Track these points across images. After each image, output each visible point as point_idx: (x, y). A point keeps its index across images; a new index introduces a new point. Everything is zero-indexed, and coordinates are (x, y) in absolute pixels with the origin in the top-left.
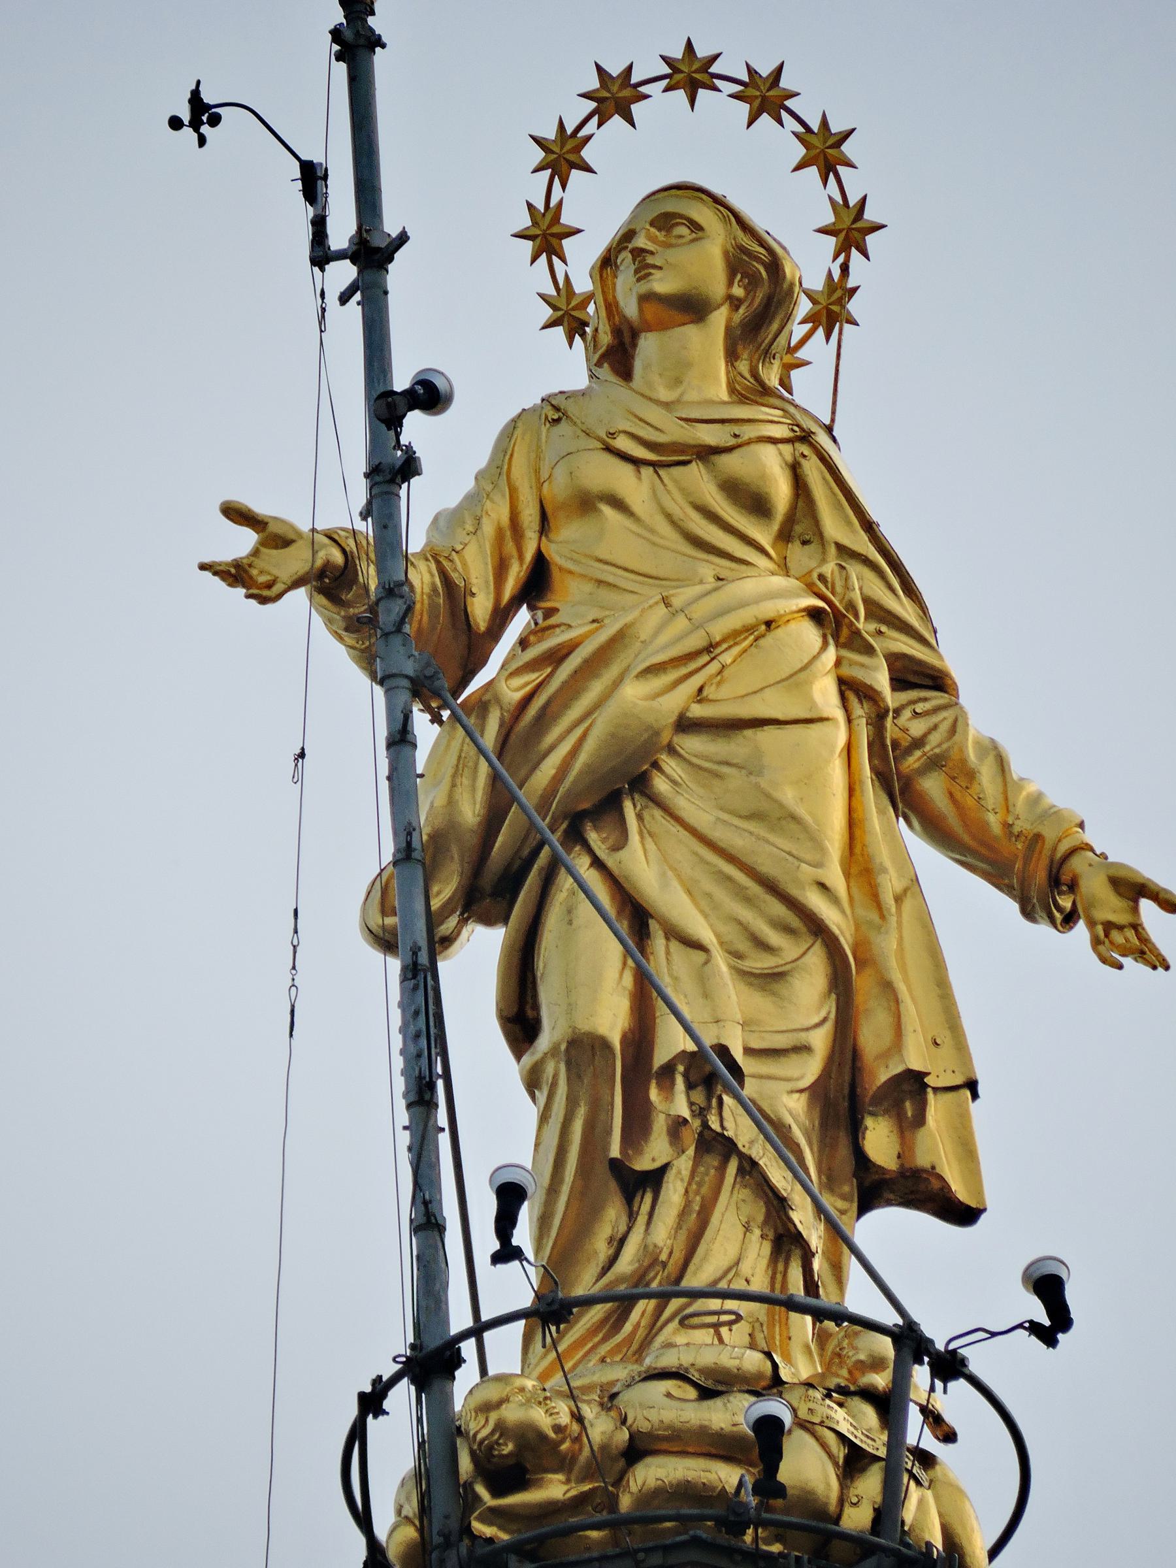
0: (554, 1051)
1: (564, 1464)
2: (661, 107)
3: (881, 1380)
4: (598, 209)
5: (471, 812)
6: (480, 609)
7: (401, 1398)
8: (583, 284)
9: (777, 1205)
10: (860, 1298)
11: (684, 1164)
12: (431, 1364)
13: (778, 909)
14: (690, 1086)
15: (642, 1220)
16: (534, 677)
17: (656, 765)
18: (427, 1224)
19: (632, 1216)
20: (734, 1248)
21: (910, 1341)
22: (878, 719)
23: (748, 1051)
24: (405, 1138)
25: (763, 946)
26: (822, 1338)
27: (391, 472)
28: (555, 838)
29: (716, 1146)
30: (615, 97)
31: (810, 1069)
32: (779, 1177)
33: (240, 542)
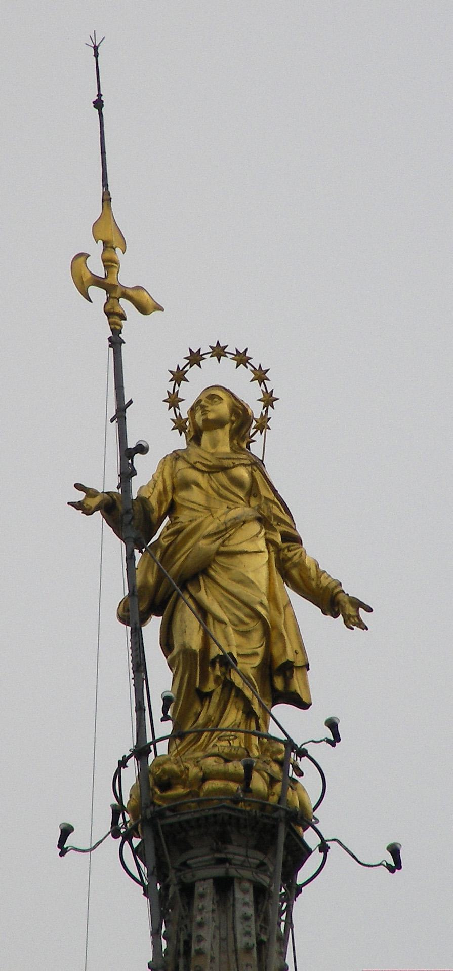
0: (178, 654)
1: (184, 784)
2: (209, 362)
3: (280, 757)
4: (190, 393)
5: (151, 580)
6: (155, 515)
7: (132, 762)
8: (185, 416)
9: (247, 703)
10: (273, 731)
11: (219, 690)
12: (141, 751)
13: (247, 611)
14: (221, 666)
15: (206, 707)
16: (172, 538)
17: (209, 566)
18: (140, 709)
19: (203, 706)
20: (233, 716)
21: (290, 744)
22: (279, 550)
23: (238, 655)
26: (260, 743)
27: (127, 474)
29: (228, 685)
30: (195, 358)
31: (257, 661)
32: (248, 693)
33: (80, 496)
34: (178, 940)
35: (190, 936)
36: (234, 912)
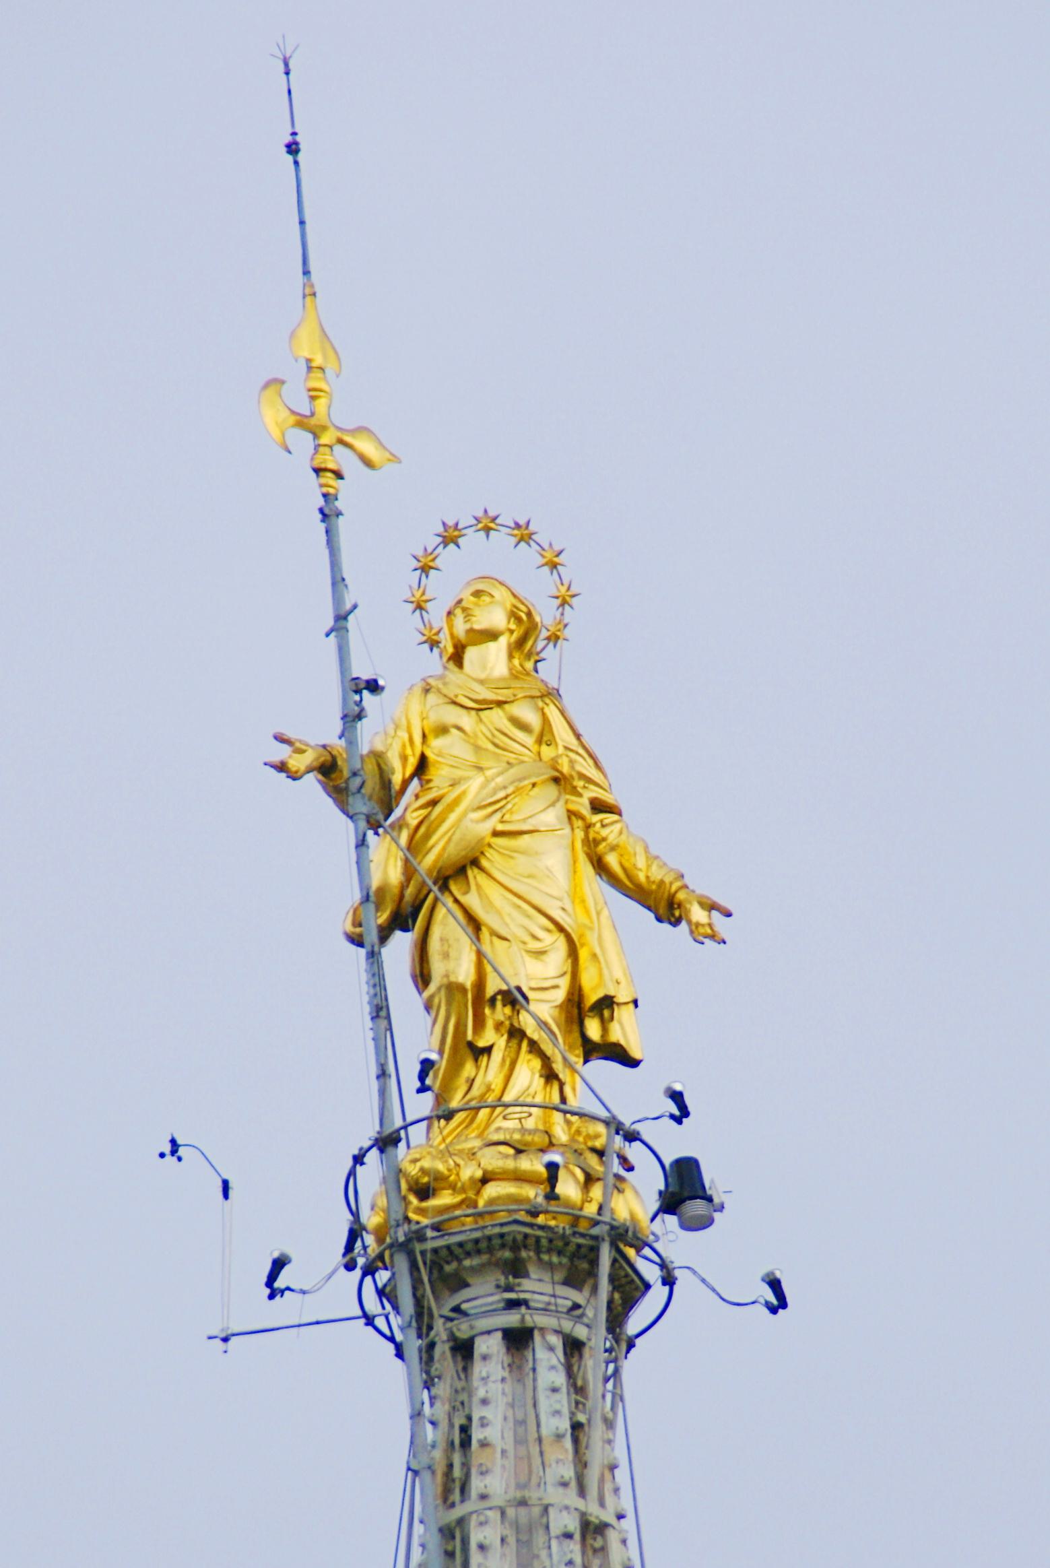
16: (424, 812)
17: (482, 853)
19: (478, 1068)
24: (371, 1034)
25: (535, 937)
28: (435, 889)
29: (516, 1034)
33: (282, 752)
34: (451, 1425)
35: (469, 1418)
36: (535, 1380)
